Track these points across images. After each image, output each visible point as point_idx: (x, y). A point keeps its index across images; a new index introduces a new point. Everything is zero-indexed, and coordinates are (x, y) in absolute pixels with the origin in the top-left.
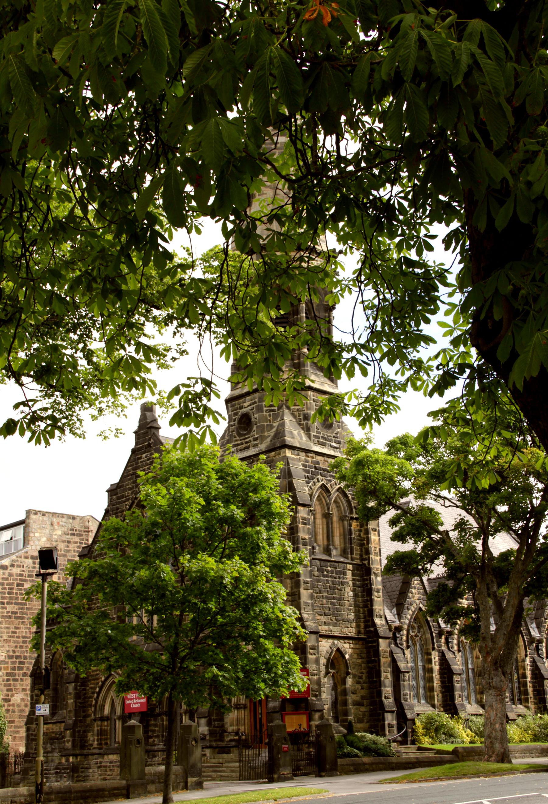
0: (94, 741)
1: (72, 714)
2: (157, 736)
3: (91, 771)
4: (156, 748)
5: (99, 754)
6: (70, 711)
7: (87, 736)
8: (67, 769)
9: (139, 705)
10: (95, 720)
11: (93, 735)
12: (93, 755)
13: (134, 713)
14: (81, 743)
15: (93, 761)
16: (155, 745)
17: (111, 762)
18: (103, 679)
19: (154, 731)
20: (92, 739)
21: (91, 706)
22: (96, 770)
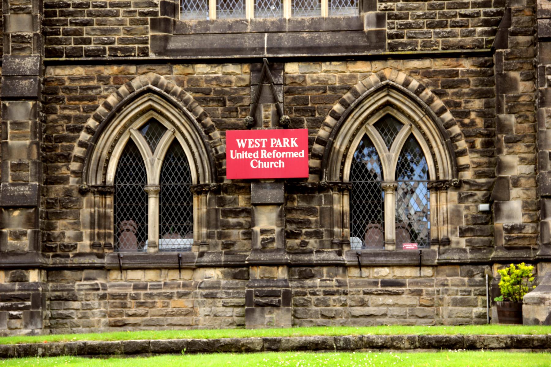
0: (79, 238)
1: (28, 174)
2: (317, 234)
3: (76, 305)
4: (314, 258)
5: (101, 268)
6: (18, 167)
7: (51, 227)
8: (24, 298)
9: (281, 164)
10: (83, 192)
11: (76, 224)
12: (80, 268)
13: (257, 181)
14: (45, 242)
15: (80, 284)
16: (311, 252)
17: (136, 287)
18: (112, 99)
19: (307, 223)
20: (76, 232)
21: (67, 158)
22: (96, 302)
